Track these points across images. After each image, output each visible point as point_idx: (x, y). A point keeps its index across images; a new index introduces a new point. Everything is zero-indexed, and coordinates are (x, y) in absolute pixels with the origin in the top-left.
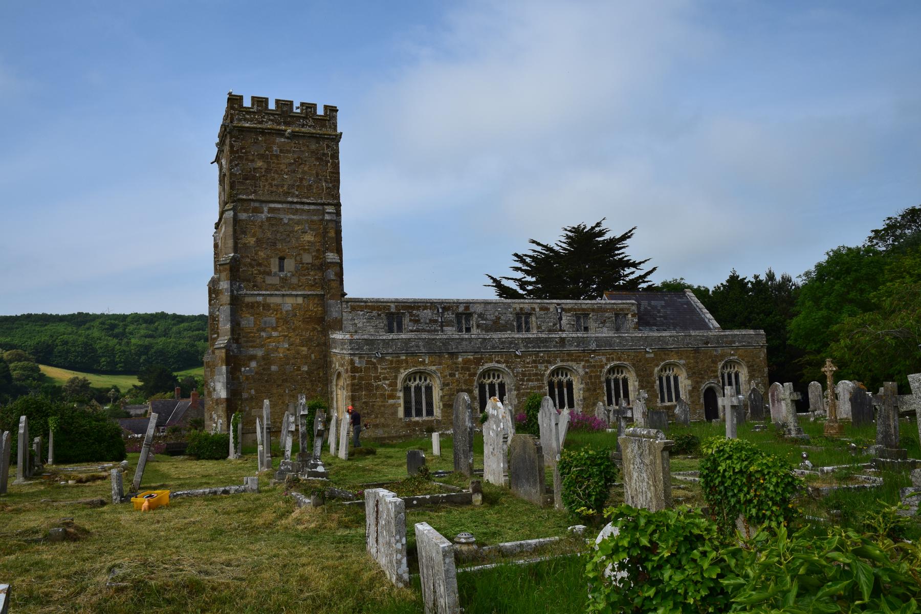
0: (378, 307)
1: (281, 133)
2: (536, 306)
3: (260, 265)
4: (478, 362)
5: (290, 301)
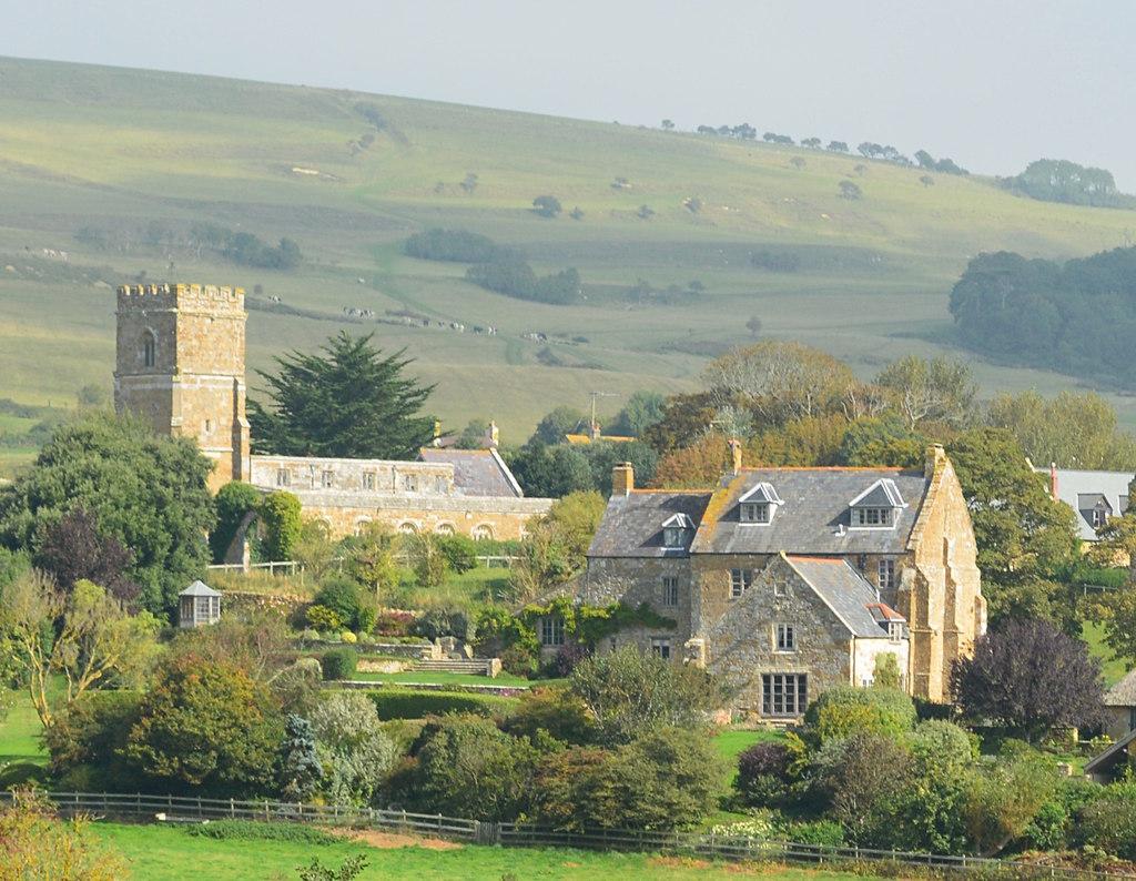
1: (207, 315)
2: (378, 467)
3: (194, 426)
4: (354, 514)
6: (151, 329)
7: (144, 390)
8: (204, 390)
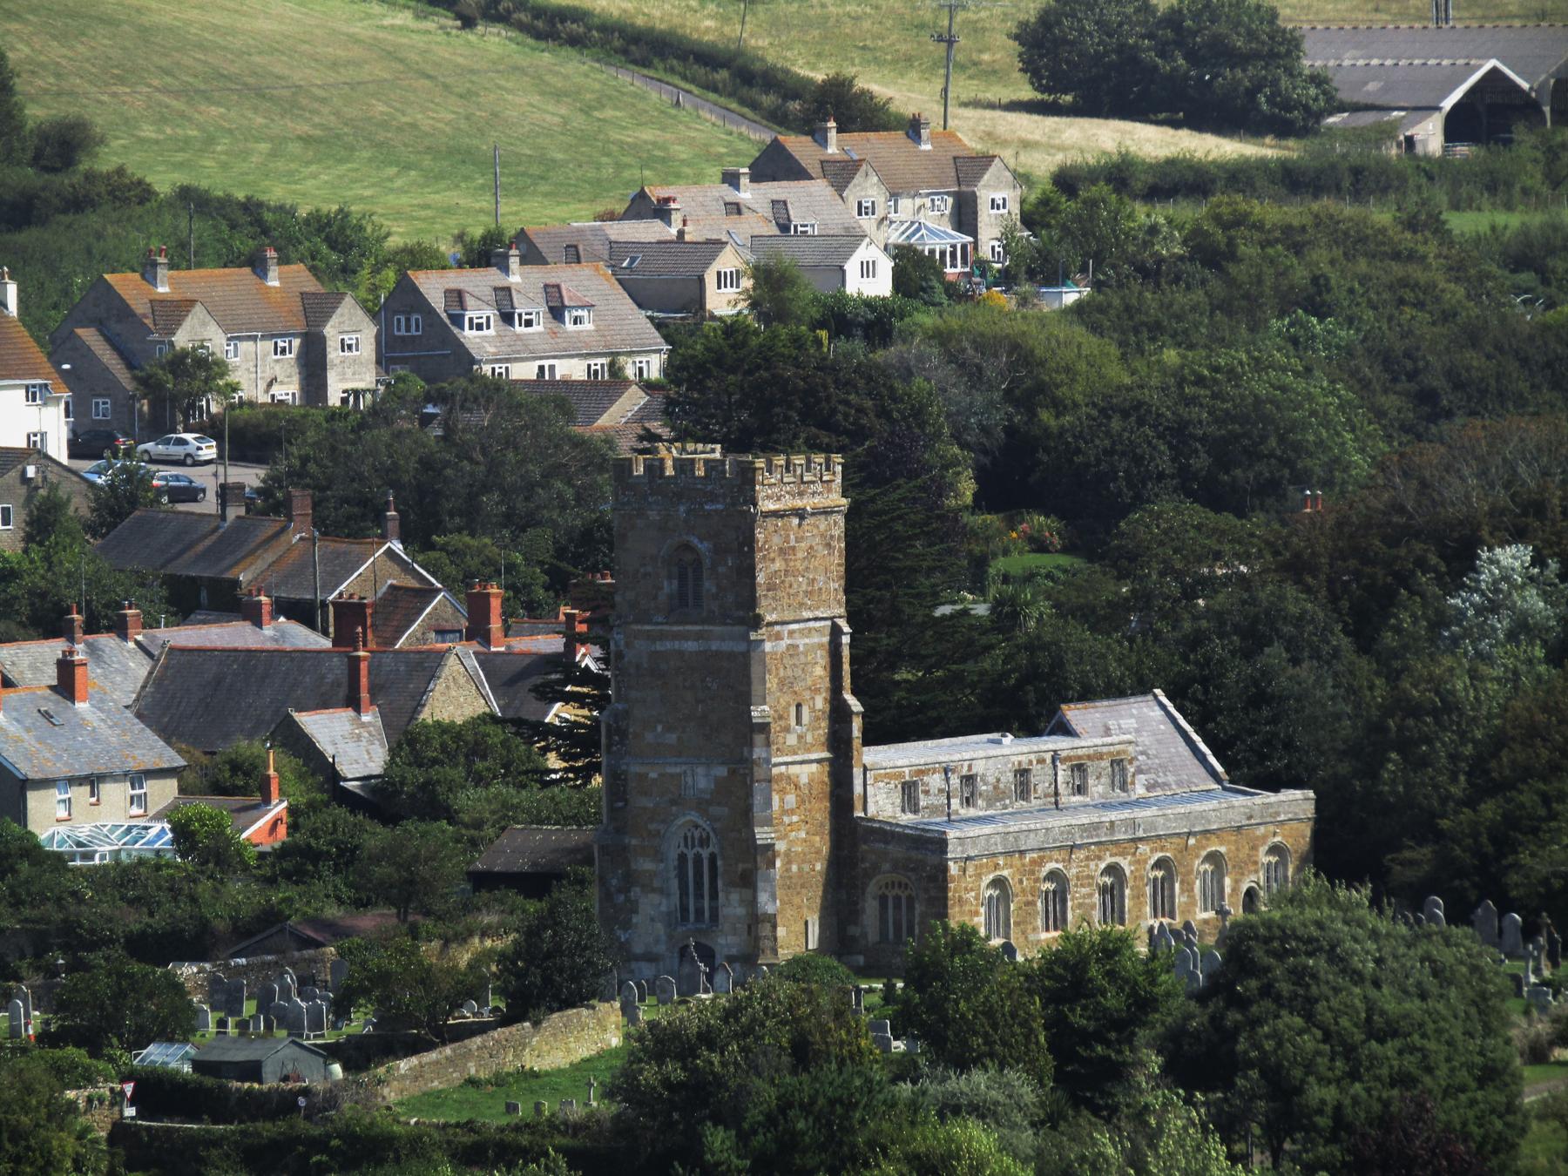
4: (1039, 862)
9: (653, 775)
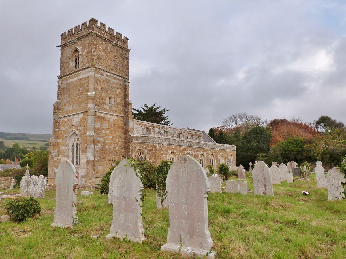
0: (144, 125)
3: (102, 99)
4: (185, 150)
5: (113, 117)
6: (77, 47)
7: (73, 82)
8: (108, 81)
9: (66, 120)
